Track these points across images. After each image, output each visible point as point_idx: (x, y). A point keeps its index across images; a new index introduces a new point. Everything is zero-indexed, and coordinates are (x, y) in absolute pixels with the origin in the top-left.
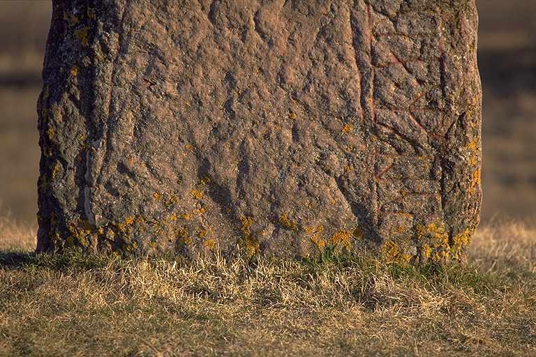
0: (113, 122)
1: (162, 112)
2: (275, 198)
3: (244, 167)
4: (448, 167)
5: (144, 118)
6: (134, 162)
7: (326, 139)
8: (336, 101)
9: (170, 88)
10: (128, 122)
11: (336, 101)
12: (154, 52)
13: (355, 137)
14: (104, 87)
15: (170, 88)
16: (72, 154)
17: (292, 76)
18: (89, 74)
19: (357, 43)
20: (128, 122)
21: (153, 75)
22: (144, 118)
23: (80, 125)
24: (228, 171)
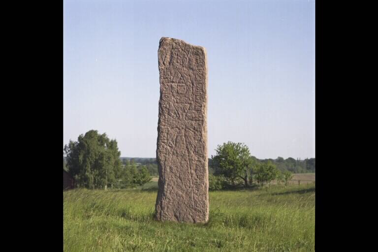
0: (164, 208)
1: (170, 207)
2: (183, 218)
3: (180, 214)
4: (205, 215)
5: (168, 207)
6: (166, 213)
7: (190, 211)
8: (191, 206)
9: (171, 204)
10: (166, 209)
11: (191, 206)
12: (169, 199)
13: (193, 211)
14: (163, 203)
15: (171, 204)
16: (159, 212)
17: (186, 203)
18: (161, 202)
19: (194, 199)
20: (166, 209)
21: (169, 202)
22: (168, 207)
23: (160, 208)
24: (178, 215)
